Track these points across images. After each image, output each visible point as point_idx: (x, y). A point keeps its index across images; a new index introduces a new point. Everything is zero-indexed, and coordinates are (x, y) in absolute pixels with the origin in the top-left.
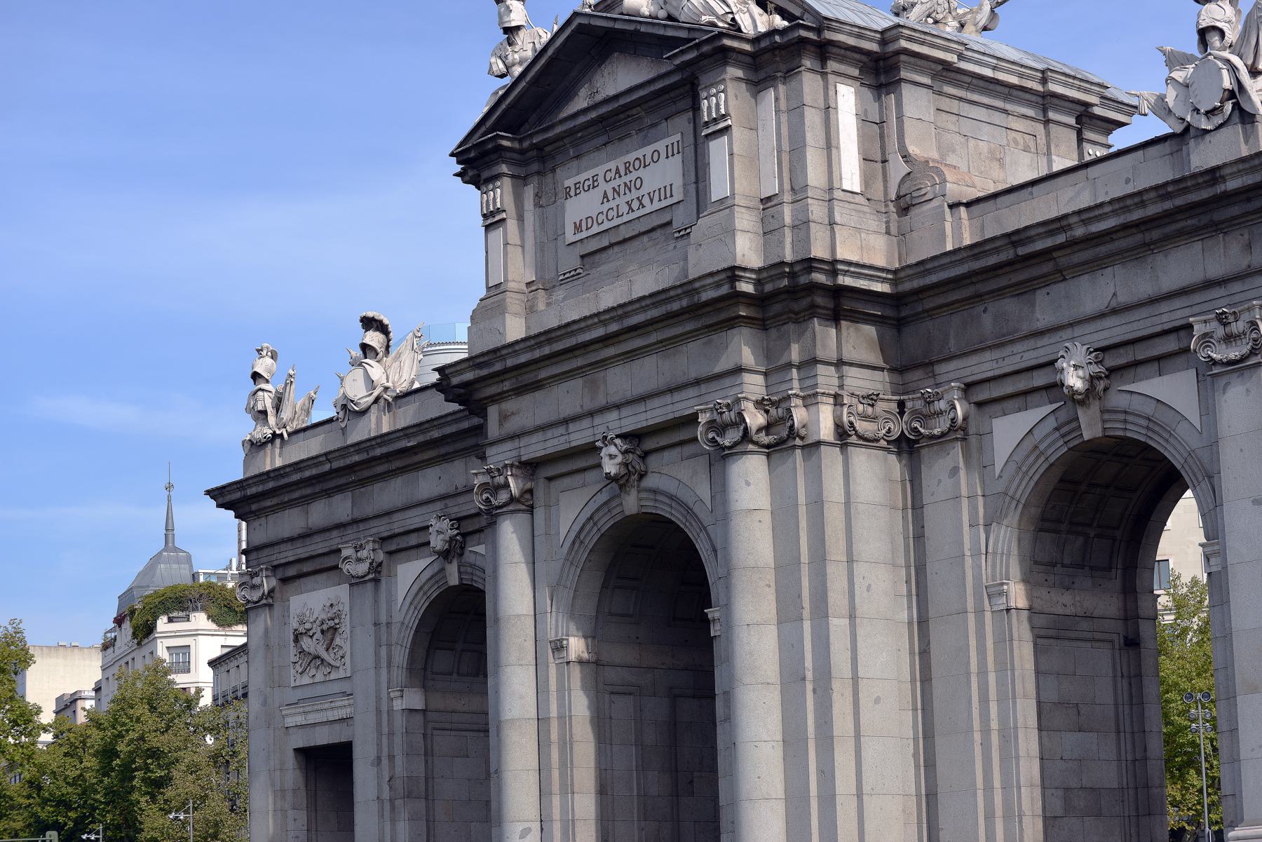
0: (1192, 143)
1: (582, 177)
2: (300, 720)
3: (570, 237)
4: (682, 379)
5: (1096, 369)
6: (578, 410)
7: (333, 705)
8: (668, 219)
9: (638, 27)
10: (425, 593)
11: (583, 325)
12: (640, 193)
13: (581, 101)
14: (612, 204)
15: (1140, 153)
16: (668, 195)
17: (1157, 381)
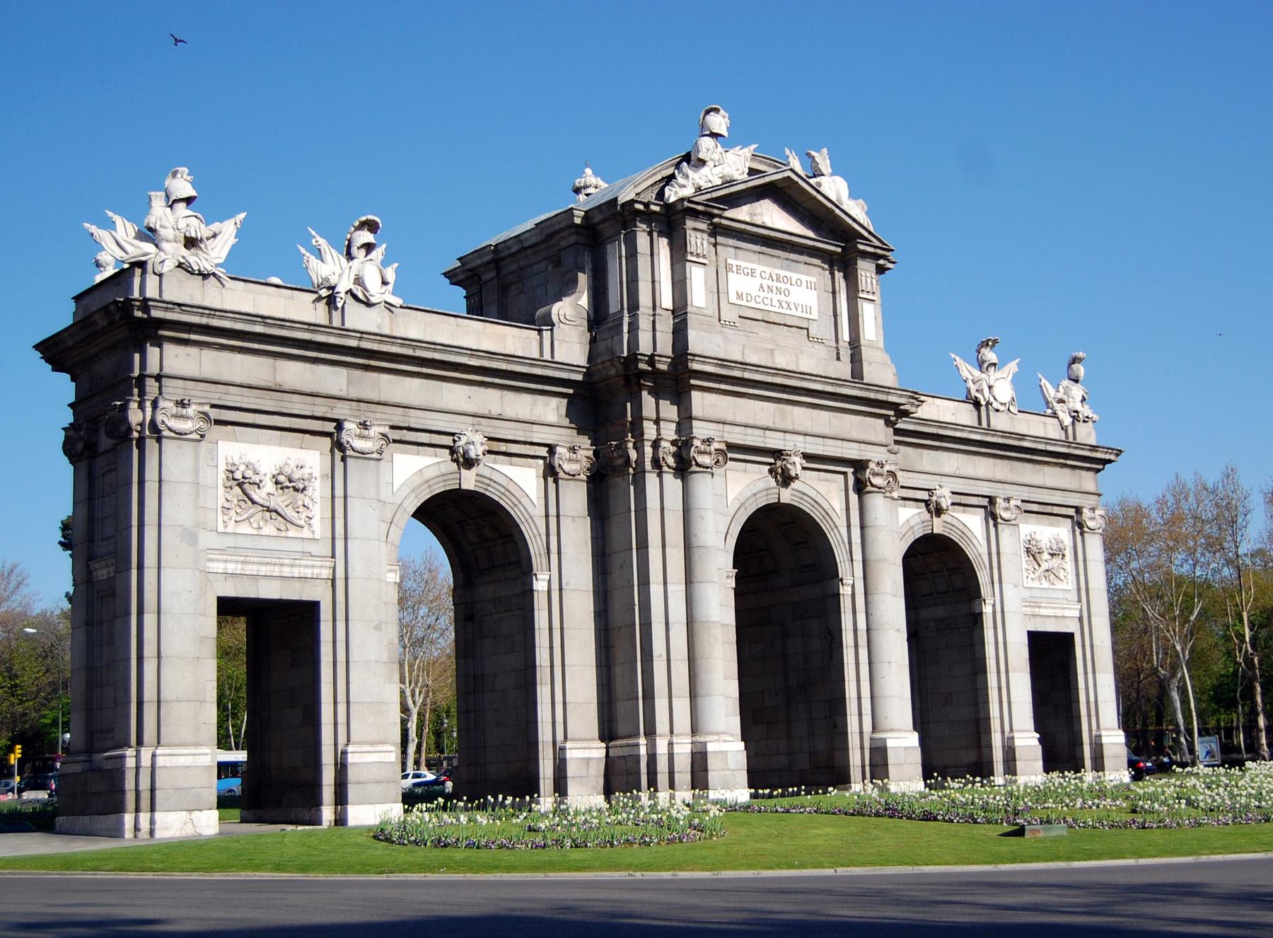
0: (992, 414)
1: (743, 264)
2: (231, 567)
3: (733, 299)
4: (847, 436)
5: (950, 502)
6: (771, 425)
7: (297, 562)
8: (806, 326)
9: (834, 208)
10: (429, 487)
11: (814, 378)
12: (787, 299)
13: (742, 213)
14: (765, 294)
15: (956, 403)
16: (809, 311)
17: (963, 515)
